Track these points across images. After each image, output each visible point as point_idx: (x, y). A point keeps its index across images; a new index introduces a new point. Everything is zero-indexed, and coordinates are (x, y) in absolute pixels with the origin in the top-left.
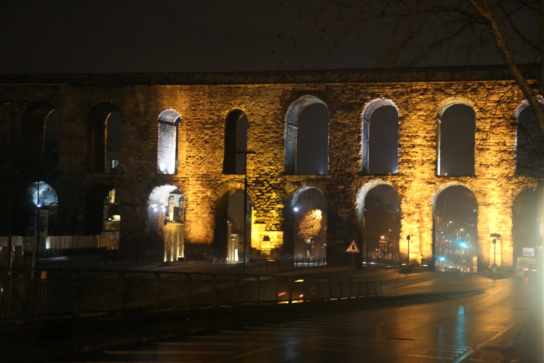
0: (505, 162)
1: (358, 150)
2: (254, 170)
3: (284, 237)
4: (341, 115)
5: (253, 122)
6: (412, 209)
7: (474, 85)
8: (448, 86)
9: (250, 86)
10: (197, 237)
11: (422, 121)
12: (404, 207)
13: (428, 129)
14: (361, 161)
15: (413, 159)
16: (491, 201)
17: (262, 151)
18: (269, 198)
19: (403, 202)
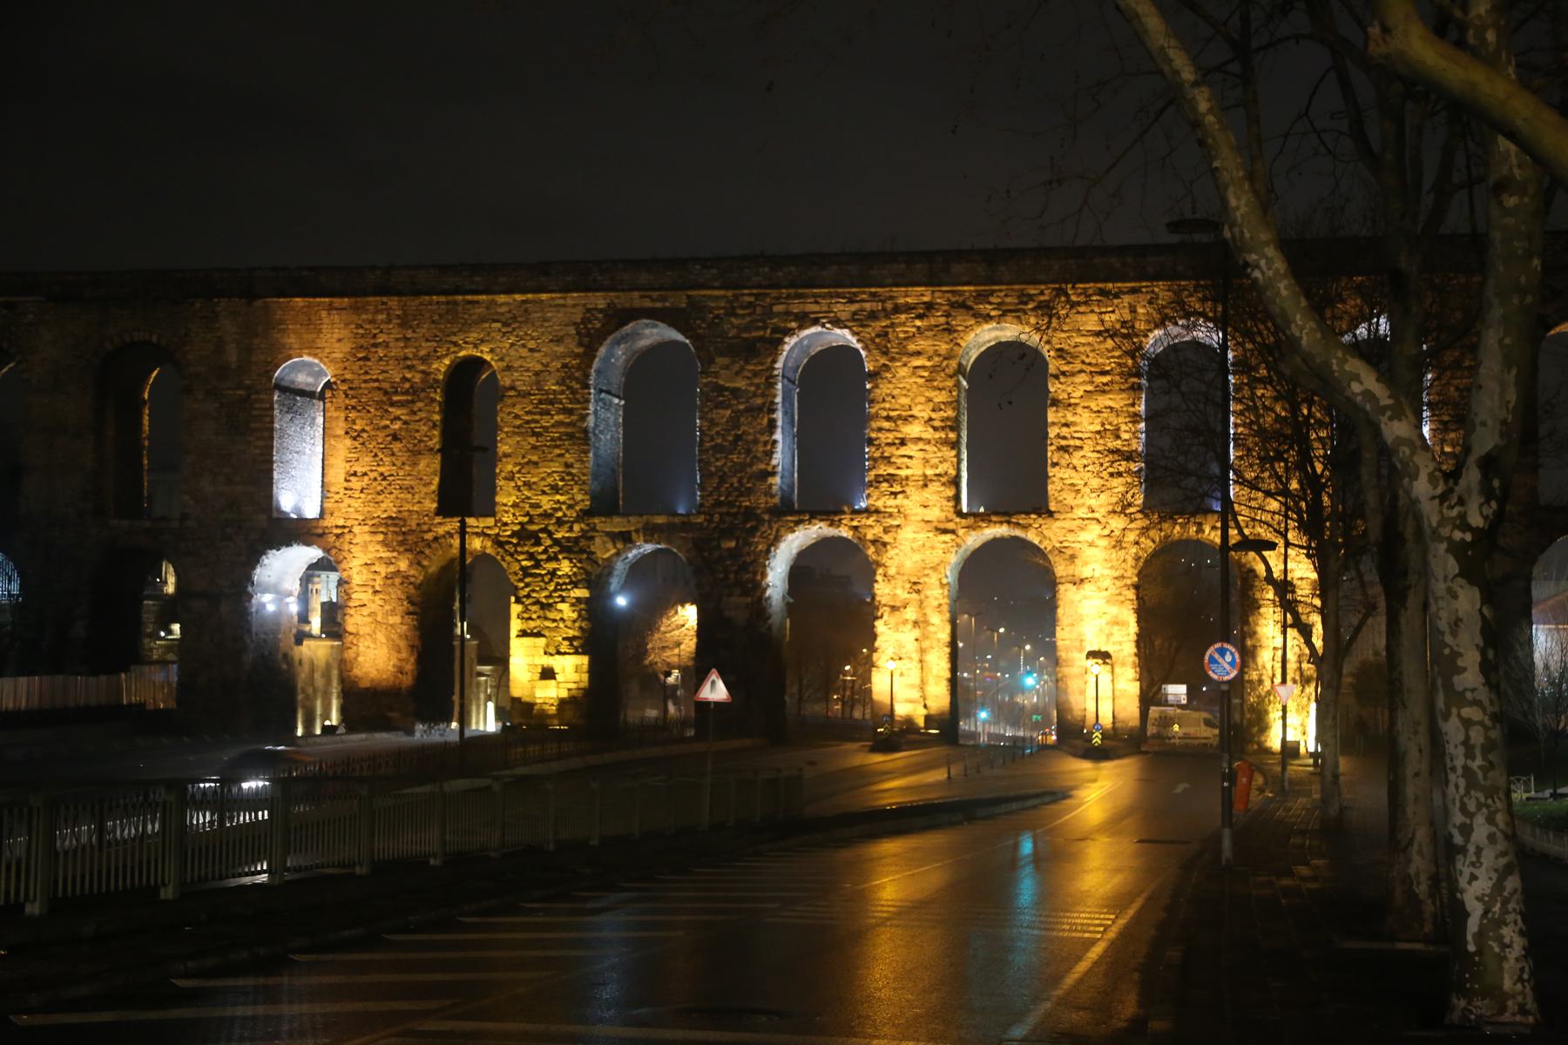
2: (515, 505)
3: (593, 670)
4: (727, 367)
5: (512, 388)
6: (902, 594)
7: (1042, 293)
8: (982, 297)
9: (502, 298)
10: (374, 674)
11: (921, 381)
12: (882, 590)
14: (777, 480)
15: (903, 473)
16: (1086, 572)
17: (535, 458)
18: (553, 573)
19: (879, 578)
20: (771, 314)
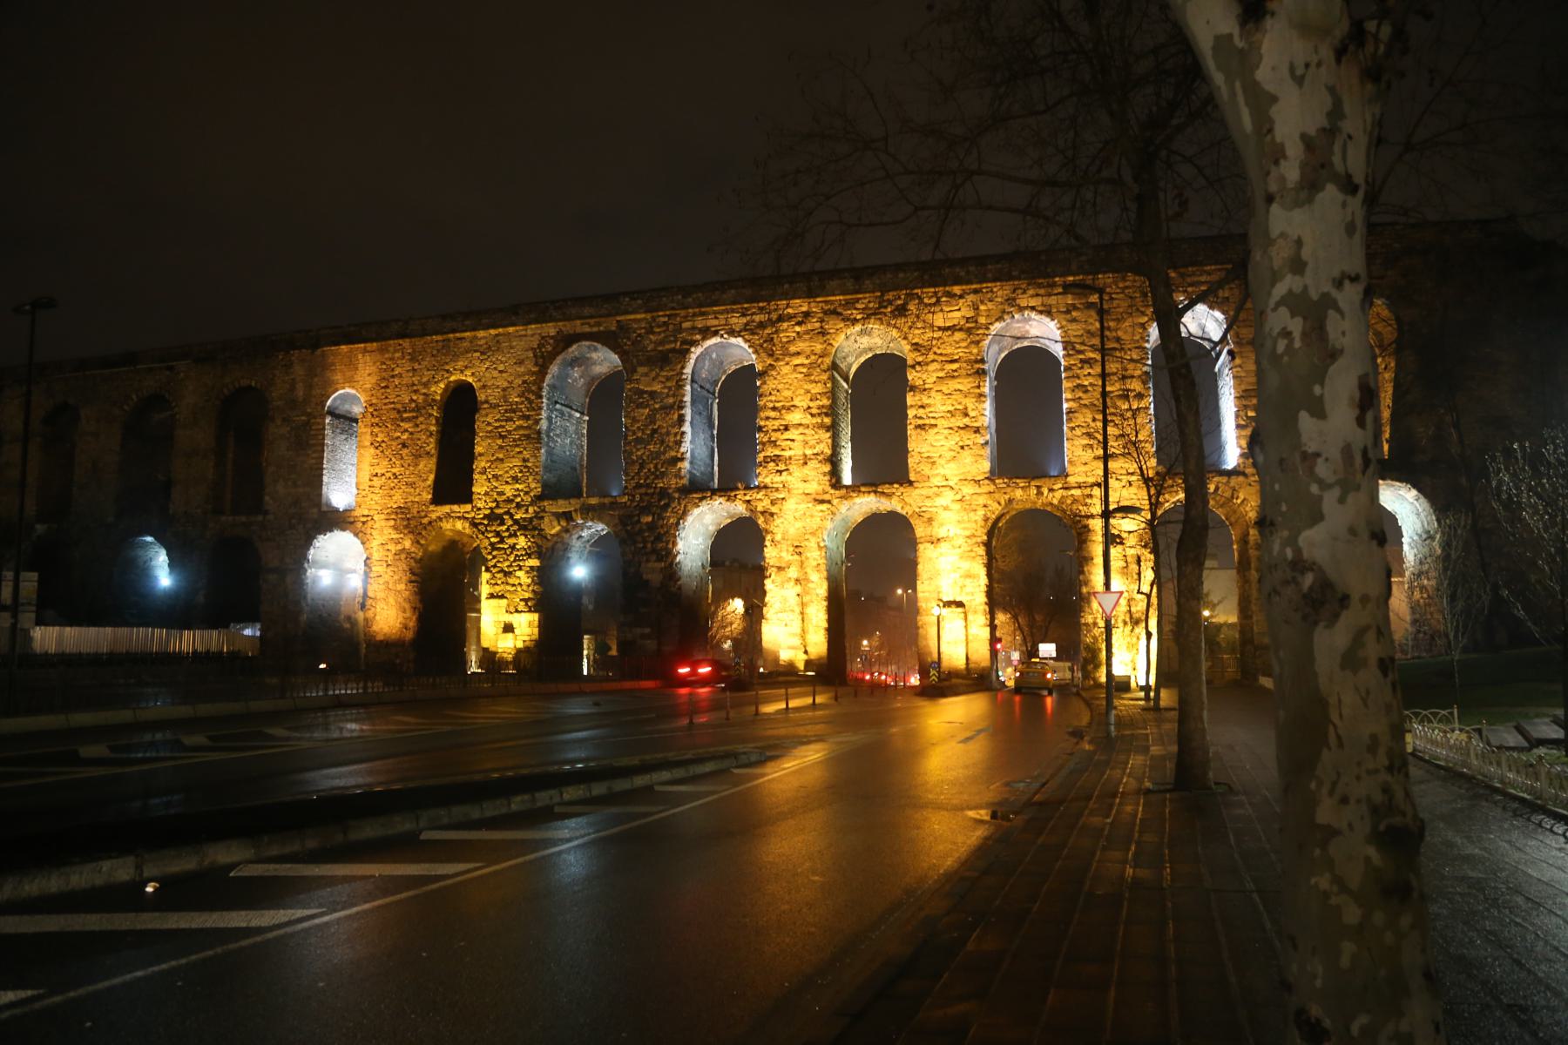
0: (966, 453)
1: (679, 443)
2: (486, 494)
3: (542, 626)
4: (646, 375)
5: (487, 402)
6: (787, 556)
8: (850, 304)
9: (481, 334)
10: (386, 629)
12: (771, 554)
14: (686, 465)
15: (787, 454)
16: (941, 533)
18: (513, 547)
20: (681, 330)
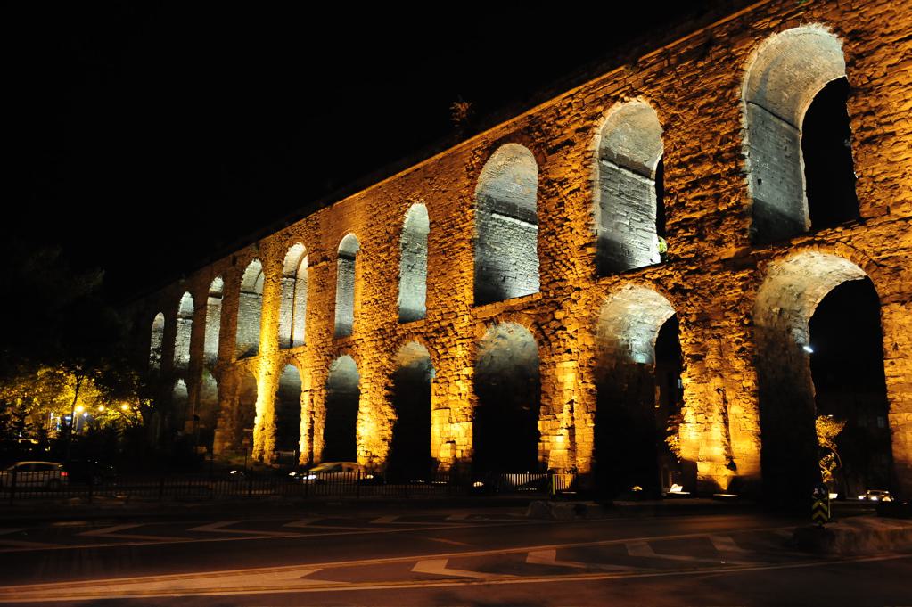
11: (706, 119)
13: (723, 133)
17: (443, 270)
19: (681, 328)
